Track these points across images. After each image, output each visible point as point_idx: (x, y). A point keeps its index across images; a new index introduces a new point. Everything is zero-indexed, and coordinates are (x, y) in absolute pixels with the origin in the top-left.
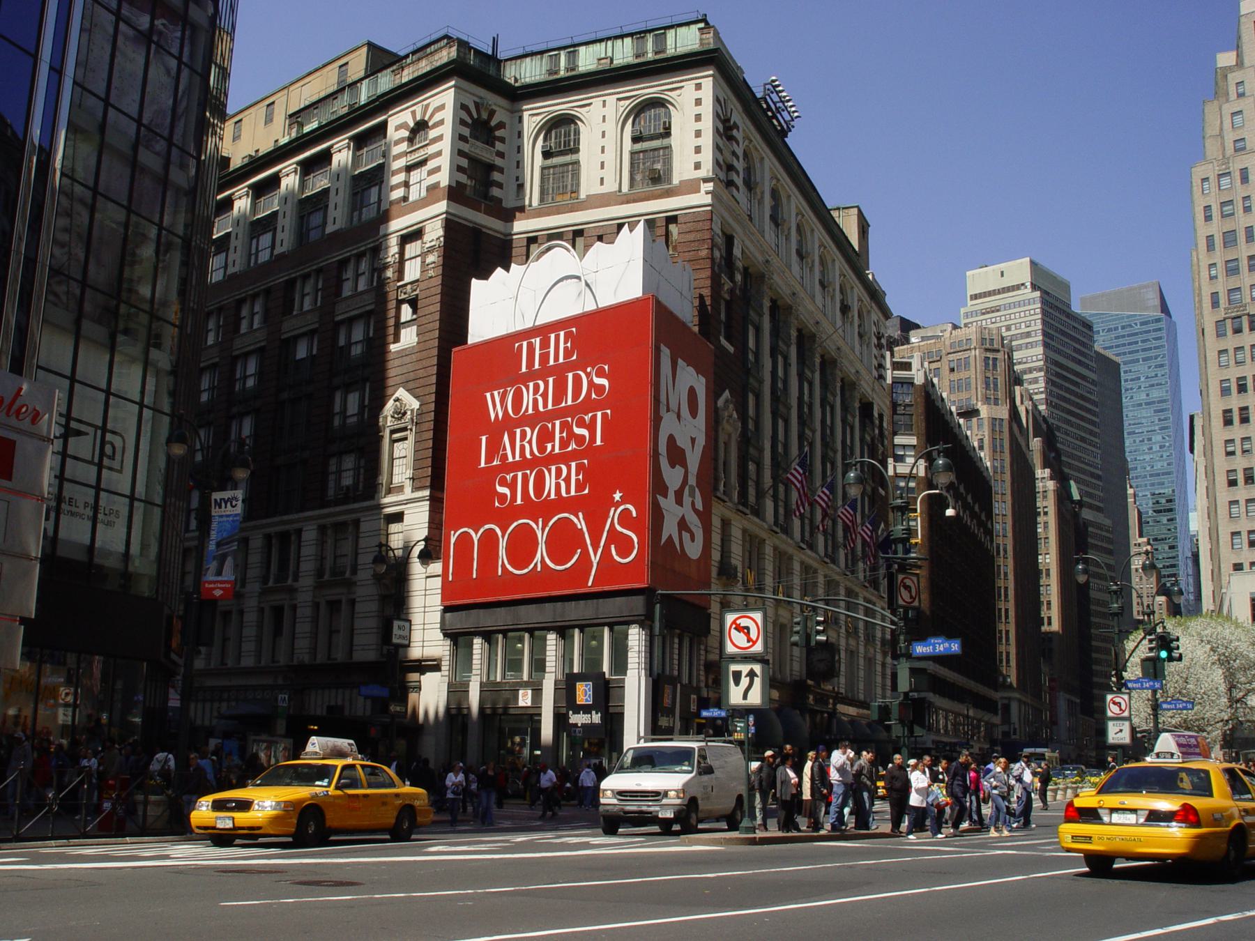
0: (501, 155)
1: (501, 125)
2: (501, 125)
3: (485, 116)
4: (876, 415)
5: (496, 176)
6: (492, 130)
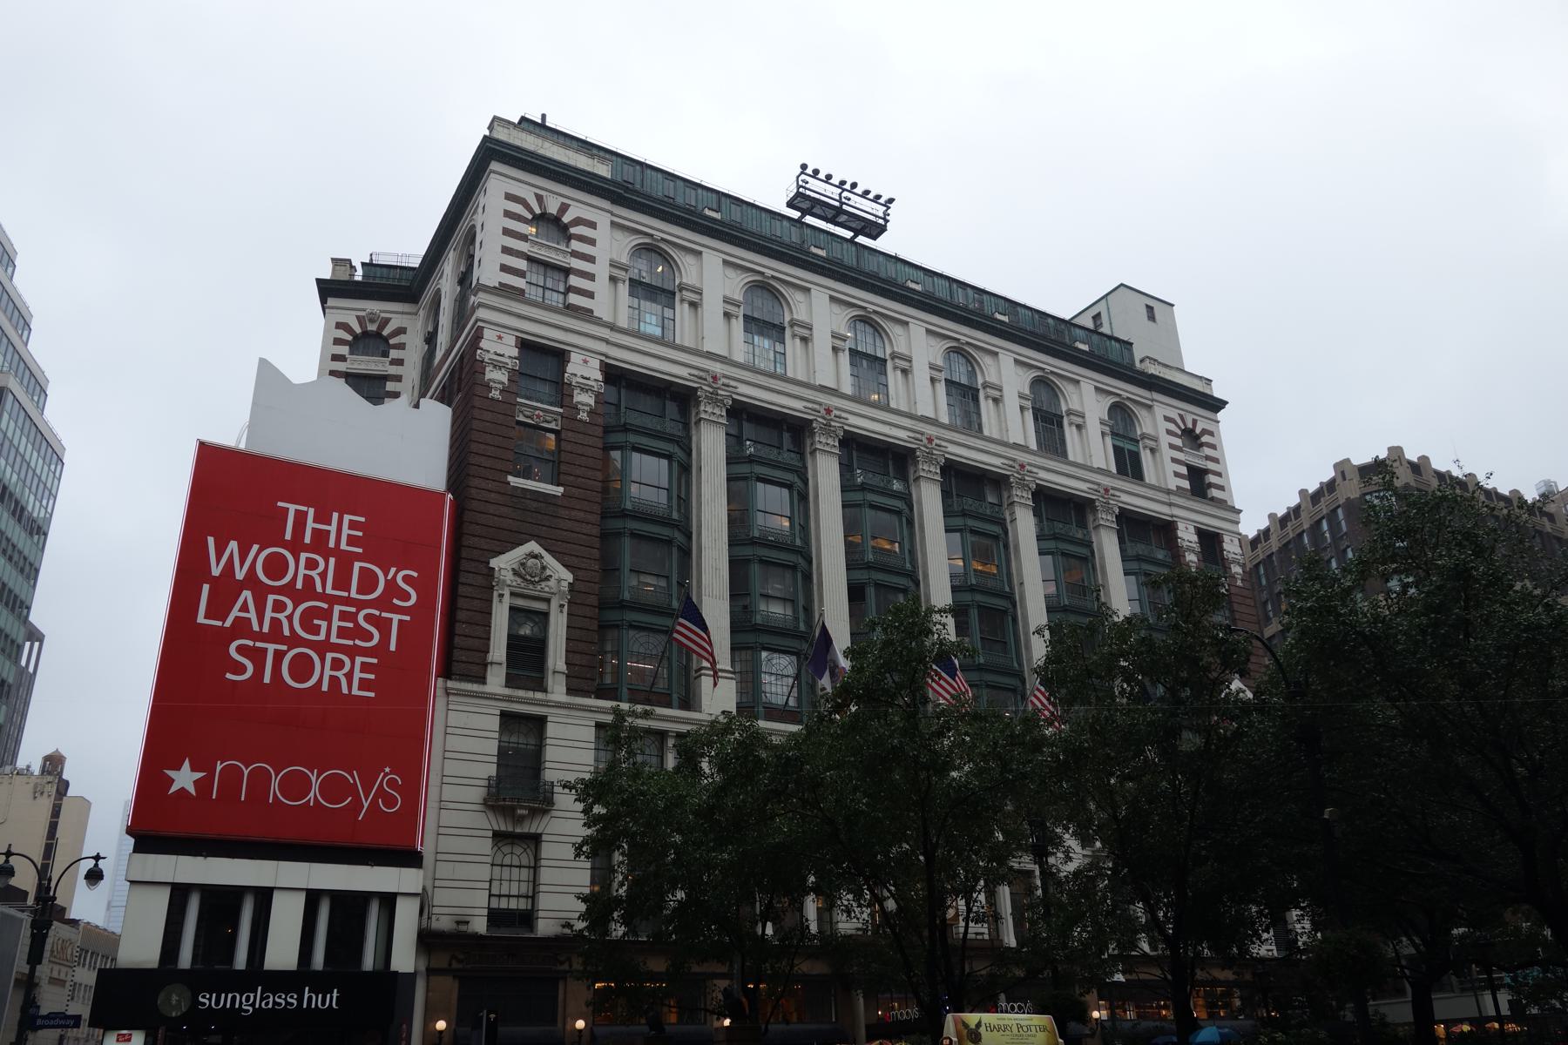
0: (400, 362)
1: (401, 331)
2: (401, 331)
3: (372, 327)
4: (1187, 535)
5: (390, 386)
6: (386, 340)
